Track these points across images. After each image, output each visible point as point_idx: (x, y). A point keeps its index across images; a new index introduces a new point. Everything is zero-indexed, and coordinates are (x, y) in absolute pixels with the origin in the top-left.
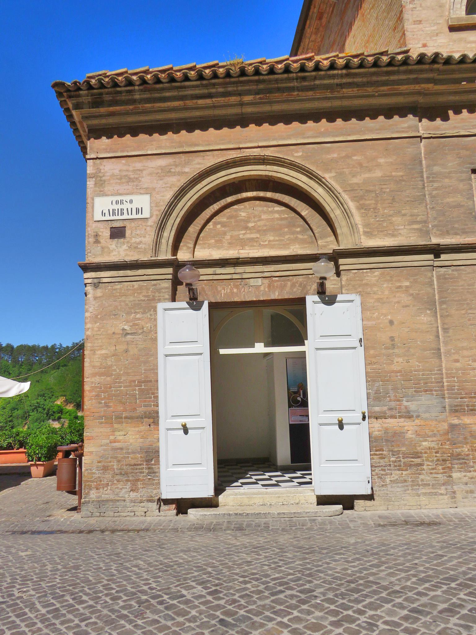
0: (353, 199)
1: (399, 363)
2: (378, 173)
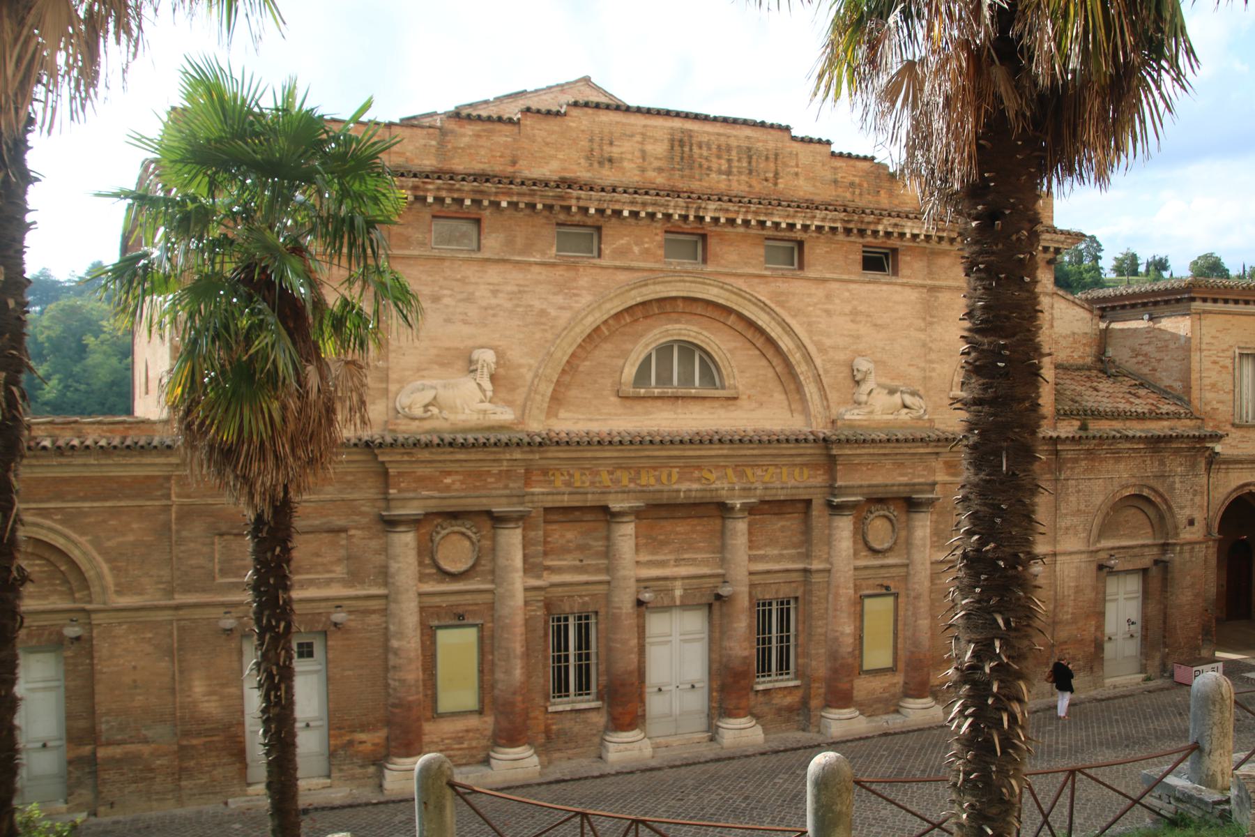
0: (108, 561)
1: (139, 700)
2: (131, 538)
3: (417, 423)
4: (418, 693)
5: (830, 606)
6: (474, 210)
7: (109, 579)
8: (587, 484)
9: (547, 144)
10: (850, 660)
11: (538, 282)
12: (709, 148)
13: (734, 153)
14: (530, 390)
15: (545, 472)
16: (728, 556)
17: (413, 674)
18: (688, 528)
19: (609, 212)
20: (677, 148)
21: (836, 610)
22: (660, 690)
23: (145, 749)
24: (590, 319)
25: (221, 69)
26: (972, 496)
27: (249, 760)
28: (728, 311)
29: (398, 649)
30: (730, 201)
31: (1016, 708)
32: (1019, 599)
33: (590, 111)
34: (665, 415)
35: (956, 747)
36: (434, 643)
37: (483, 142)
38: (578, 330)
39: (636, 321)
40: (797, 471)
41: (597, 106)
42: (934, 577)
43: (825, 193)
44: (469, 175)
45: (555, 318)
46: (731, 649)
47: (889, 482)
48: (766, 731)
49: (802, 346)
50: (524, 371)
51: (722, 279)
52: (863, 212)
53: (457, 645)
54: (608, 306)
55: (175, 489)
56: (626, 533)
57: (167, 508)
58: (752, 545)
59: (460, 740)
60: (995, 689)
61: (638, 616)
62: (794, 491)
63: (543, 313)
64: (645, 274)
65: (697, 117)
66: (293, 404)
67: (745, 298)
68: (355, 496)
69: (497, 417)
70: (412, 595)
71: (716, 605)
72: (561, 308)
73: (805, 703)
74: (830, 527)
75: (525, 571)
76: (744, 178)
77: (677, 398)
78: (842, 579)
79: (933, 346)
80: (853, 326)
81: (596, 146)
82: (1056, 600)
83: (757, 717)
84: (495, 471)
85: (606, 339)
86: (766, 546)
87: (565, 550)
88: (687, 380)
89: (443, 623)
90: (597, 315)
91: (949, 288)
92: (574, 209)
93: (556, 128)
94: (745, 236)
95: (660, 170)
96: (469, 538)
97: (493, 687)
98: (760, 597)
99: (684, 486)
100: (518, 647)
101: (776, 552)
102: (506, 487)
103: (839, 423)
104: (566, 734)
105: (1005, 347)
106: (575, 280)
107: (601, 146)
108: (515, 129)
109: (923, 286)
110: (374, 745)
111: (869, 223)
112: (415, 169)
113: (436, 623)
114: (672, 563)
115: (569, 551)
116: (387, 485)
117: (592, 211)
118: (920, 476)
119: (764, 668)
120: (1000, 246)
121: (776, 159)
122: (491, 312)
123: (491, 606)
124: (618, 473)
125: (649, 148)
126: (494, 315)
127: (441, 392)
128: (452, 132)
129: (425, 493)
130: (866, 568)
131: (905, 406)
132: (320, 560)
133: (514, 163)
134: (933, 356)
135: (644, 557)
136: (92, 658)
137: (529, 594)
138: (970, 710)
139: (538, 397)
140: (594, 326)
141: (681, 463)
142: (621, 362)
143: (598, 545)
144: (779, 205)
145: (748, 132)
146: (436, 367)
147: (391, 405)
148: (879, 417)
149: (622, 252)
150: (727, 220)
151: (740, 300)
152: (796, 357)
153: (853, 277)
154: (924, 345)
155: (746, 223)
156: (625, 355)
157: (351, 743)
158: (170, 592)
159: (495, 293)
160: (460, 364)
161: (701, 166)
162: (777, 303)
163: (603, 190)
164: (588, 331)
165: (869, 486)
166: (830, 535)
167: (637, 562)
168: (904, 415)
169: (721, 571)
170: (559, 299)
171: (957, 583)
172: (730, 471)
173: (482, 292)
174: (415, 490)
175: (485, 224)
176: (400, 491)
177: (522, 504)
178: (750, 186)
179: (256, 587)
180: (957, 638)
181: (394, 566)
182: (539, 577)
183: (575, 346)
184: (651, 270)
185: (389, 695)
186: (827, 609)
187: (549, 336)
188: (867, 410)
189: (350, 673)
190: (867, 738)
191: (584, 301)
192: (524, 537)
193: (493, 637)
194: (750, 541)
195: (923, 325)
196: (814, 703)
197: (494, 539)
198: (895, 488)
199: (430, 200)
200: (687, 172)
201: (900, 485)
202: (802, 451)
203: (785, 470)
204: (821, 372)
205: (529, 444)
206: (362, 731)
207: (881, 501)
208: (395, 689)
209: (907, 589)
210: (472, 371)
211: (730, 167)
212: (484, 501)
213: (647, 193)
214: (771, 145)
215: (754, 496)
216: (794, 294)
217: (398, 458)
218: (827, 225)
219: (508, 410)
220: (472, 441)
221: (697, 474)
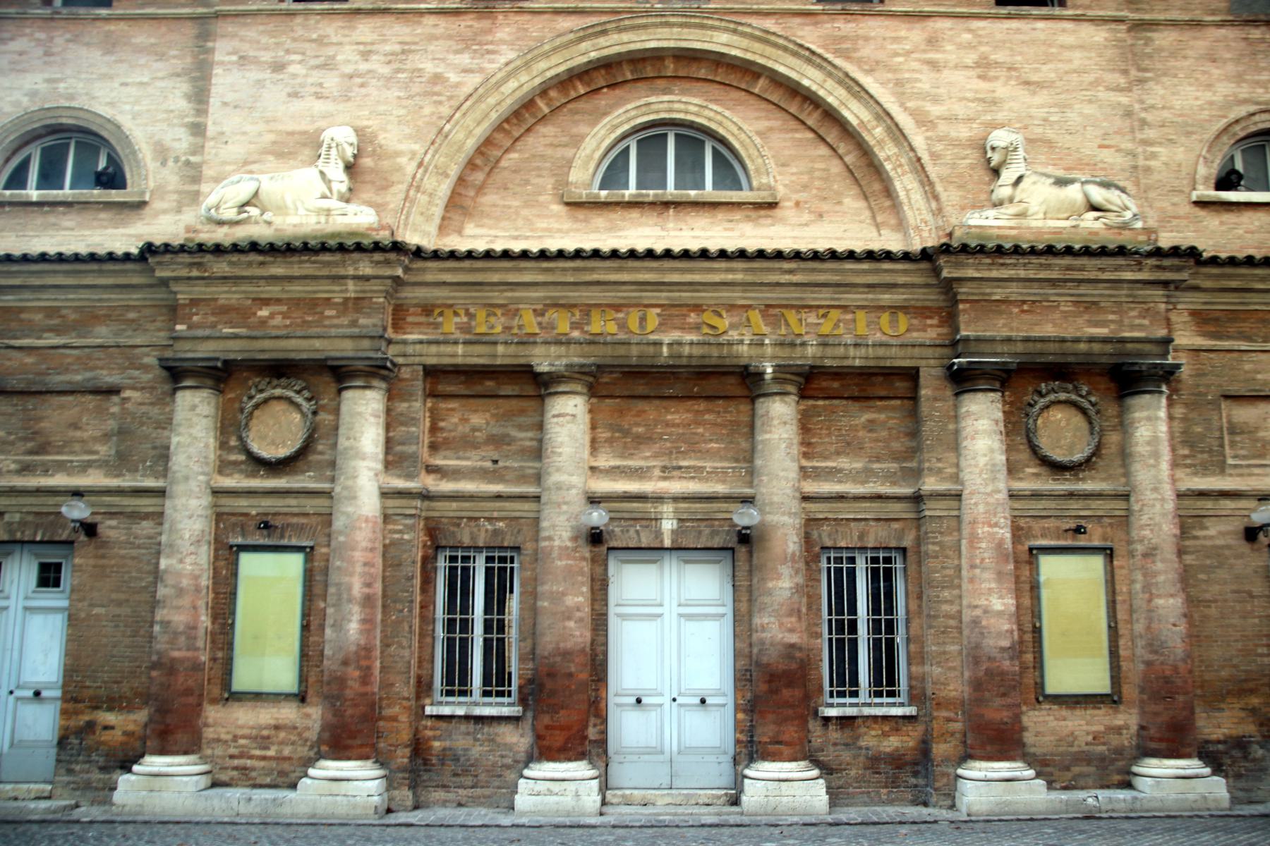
3: (225, 229)
5: (964, 562)
8: (499, 329)
11: (432, 38)
15: (428, 309)
18: (688, 416)
21: (973, 567)
22: (639, 701)
24: (513, 84)
34: (647, 231)
38: (492, 100)
39: (597, 91)
42: (1187, 524)
45: (457, 85)
46: (763, 629)
47: (1069, 333)
48: (836, 797)
49: (884, 115)
50: (403, 160)
53: (271, 580)
54: (543, 65)
56: (569, 416)
58: (808, 447)
59: (264, 742)
61: (593, 560)
62: (881, 352)
63: (437, 78)
64: (604, 19)
67: (776, 45)
68: (138, 341)
72: (466, 71)
74: (956, 418)
77: (666, 205)
79: (1149, 117)
83: (827, 770)
86: (838, 453)
87: (467, 443)
89: (250, 541)
90: (524, 78)
91: (1173, 24)
96: (298, 406)
98: (829, 543)
101: (858, 465)
104: (456, 759)
106: (490, 31)
110: (125, 733)
113: (239, 540)
114: (657, 472)
115: (475, 446)
118: (1133, 327)
119: (845, 681)
122: (359, 80)
123: (327, 519)
124: (552, 315)
126: (362, 85)
130: (1036, 495)
131: (1094, 208)
132: (78, 434)
134: (1151, 134)
135: (605, 460)
137: (390, 503)
139: (423, 198)
141: (663, 296)
142: (569, 152)
143: (525, 438)
146: (271, 158)
148: (1036, 223)
151: (769, 50)
152: (875, 134)
154: (1128, 114)
156: (577, 141)
157: (91, 726)
162: (837, 52)
164: (509, 101)
165: (1027, 340)
166: (957, 432)
167: (592, 469)
168: (1090, 221)
169: (748, 491)
170: (465, 59)
172: (755, 316)
173: (347, 57)
176: (190, 328)
182: (409, 476)
184: (614, 12)
186: (959, 568)
187: (445, 110)
191: (503, 60)
192: (388, 411)
194: (804, 443)
195: (1122, 81)
196: (940, 749)
198: (1083, 347)
201: (1091, 340)
202: (888, 279)
203: (861, 315)
204: (926, 158)
206: (110, 709)
209: (1130, 542)
212: (317, 344)
216: (867, 39)
217: (184, 273)
221: (693, 318)
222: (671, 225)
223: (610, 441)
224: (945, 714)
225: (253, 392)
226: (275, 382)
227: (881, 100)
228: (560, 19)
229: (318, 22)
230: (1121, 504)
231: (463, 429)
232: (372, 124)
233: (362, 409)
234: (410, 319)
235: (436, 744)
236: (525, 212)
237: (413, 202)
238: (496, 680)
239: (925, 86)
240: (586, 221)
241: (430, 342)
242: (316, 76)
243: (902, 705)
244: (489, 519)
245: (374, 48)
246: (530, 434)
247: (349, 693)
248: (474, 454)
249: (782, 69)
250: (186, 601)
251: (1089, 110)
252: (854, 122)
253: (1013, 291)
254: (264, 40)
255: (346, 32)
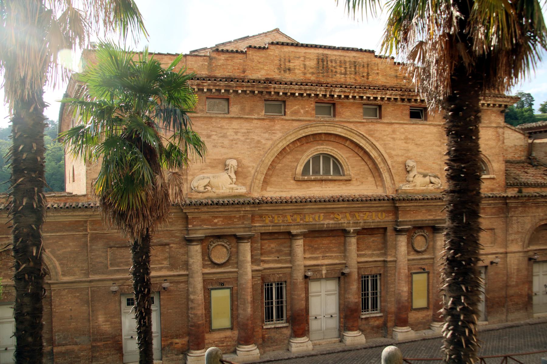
2: (69, 249)
4: (203, 320)
5: (396, 278)
6: (226, 94)
7: (59, 269)
8: (281, 221)
9: (260, 63)
10: (407, 304)
12: (336, 63)
13: (348, 64)
14: (253, 178)
15: (261, 216)
16: (347, 254)
17: (200, 311)
19: (289, 94)
20: (320, 63)
21: (399, 280)
22: (316, 318)
23: (76, 348)
24: (281, 144)
25: (115, 45)
26: (450, 233)
27: (124, 352)
28: (346, 139)
29: (194, 299)
30: (346, 87)
31: (472, 326)
32: (472, 278)
33: (279, 46)
34: (317, 188)
35: (445, 343)
36: (210, 296)
37: (229, 62)
38: (275, 149)
39: (303, 144)
40: (380, 214)
41: (283, 44)
43: (392, 82)
44: (224, 78)
45: (265, 144)
46: (349, 298)
47: (424, 219)
49: (381, 155)
50: (250, 169)
51: (343, 124)
52: (410, 91)
54: (289, 138)
55: (89, 227)
56: (299, 244)
57: (86, 235)
59: (222, 342)
60: (462, 318)
61: (305, 283)
62: (378, 224)
63: (259, 142)
65: (330, 48)
66: (150, 192)
67: (353, 133)
68: (173, 228)
69: (238, 191)
70: (200, 274)
71: (342, 277)
72: (267, 139)
73: (385, 324)
74: (396, 240)
75: (252, 262)
76: (352, 76)
77: (322, 180)
78: (402, 265)
80: (406, 145)
81: (282, 63)
82: (507, 275)
83: (362, 331)
84: (238, 216)
85: (288, 154)
86: (365, 249)
87: (270, 253)
88: (327, 172)
89: (214, 287)
90: (284, 142)
92: (273, 93)
93: (263, 55)
94: (353, 104)
95: (313, 73)
96: (226, 247)
97: (237, 317)
98: (363, 274)
99: (326, 222)
100: (249, 299)
102: (243, 223)
103: (400, 191)
105: (464, 168)
106: (273, 126)
107: (285, 63)
108: (245, 56)
109: (439, 125)
110: (182, 344)
111: (413, 96)
112: (198, 76)
113: (211, 287)
114: (321, 258)
115: (272, 253)
116: (187, 224)
117: (281, 94)
118: (439, 216)
119: (365, 307)
120: (462, 123)
121: (368, 66)
123: (237, 279)
124: (295, 216)
125: (307, 63)
126: (236, 144)
127: (212, 180)
128: (215, 58)
129: (205, 227)
130: (413, 260)
131: (431, 183)
132: (157, 258)
133: (244, 72)
135: (308, 256)
136: (51, 305)
137: (254, 273)
138: (451, 327)
139: (257, 181)
140: (283, 147)
141: (324, 211)
143: (286, 250)
144: (370, 89)
145: (354, 54)
146: (209, 168)
147: (189, 186)
149: (296, 113)
150: (345, 96)
151: (352, 134)
152: (378, 160)
153: (405, 122)
155: (354, 97)
156: (298, 161)
157: (171, 344)
158: (87, 274)
159: (236, 133)
160: (221, 166)
161: (332, 71)
163: (286, 84)
165: (415, 221)
166: (396, 244)
167: (305, 258)
169: (344, 262)
170: (266, 135)
171: (444, 271)
172: (348, 215)
173: (230, 133)
174: (200, 225)
175: (231, 101)
176: (193, 226)
177: (250, 231)
178: (356, 80)
179: (134, 274)
180: (445, 295)
181: (191, 261)
182: (259, 265)
183: (274, 157)
184: (309, 121)
185: (189, 321)
186: (395, 279)
187: (262, 153)
188: (413, 185)
189: (171, 311)
190: (415, 341)
192: (251, 246)
193: (237, 293)
194: (358, 247)
195: (439, 143)
196: (389, 324)
197: (237, 247)
198: (427, 222)
199: (205, 90)
200: (325, 74)
201: (429, 220)
202: (382, 205)
203: (374, 213)
204: (391, 167)
205: (253, 203)
206: (177, 338)
207: (420, 228)
208: (192, 318)
209: (434, 270)
210: (226, 170)
211: (346, 71)
212: (233, 230)
213: (307, 85)
214: (365, 60)
215: (359, 226)
216: (377, 130)
217: (193, 211)
218: (393, 97)
219: (244, 188)
220: (227, 202)
221: (332, 216)
222: (323, 186)
223: (308, 250)
224: (390, 316)
225: (212, 243)
226: (219, 240)
227: (380, 150)
228: (294, 122)
229: (220, 121)
230: (432, 260)
231: (269, 249)
232: (240, 157)
233: (247, 249)
234: (256, 219)
235: (266, 336)
236: (283, 183)
237: (255, 183)
238: (280, 316)
239: (391, 145)
240: (301, 185)
241: (262, 226)
242: (221, 140)
243: (379, 313)
244: (278, 274)
245: (238, 131)
246: (287, 249)
247: (249, 328)
248: (272, 255)
249: (355, 140)
250: (200, 308)
251: (431, 152)
252: (373, 157)
253: (412, 208)
254: (203, 126)
255: (229, 125)
